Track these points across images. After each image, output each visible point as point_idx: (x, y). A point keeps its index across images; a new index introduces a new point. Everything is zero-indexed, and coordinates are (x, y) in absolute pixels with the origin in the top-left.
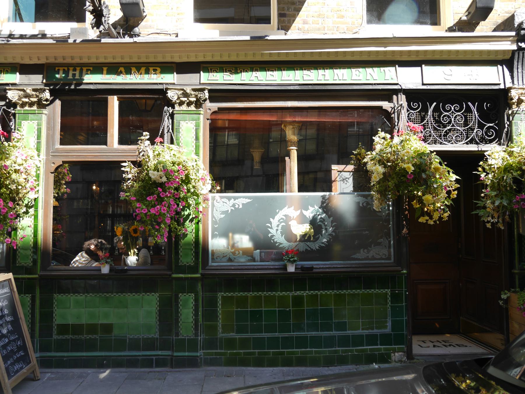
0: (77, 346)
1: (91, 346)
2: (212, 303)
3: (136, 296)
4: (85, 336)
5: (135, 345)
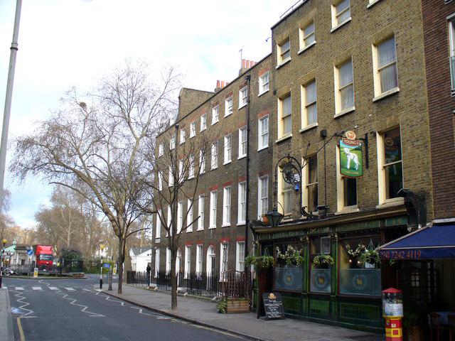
0: (313, 316)
2: (338, 306)
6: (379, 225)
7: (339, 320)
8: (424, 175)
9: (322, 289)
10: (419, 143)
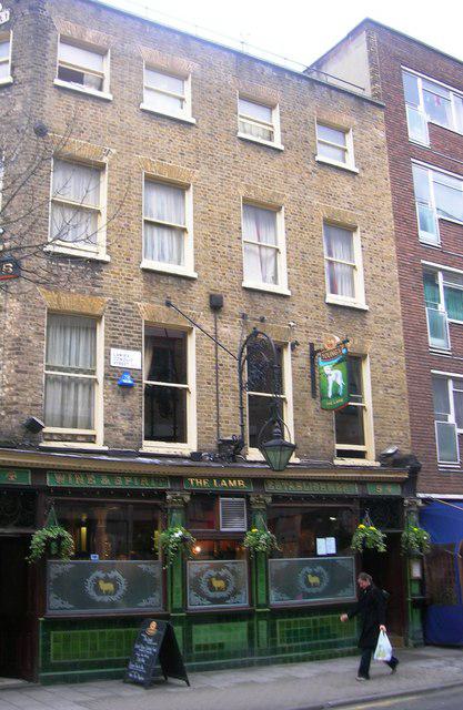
0: (205, 658)
1: (213, 657)
2: (275, 625)
3: (236, 624)
4: (210, 651)
5: (235, 654)
6: (355, 490)
7: (274, 651)
8: (401, 434)
9: (222, 600)
10: (393, 391)
